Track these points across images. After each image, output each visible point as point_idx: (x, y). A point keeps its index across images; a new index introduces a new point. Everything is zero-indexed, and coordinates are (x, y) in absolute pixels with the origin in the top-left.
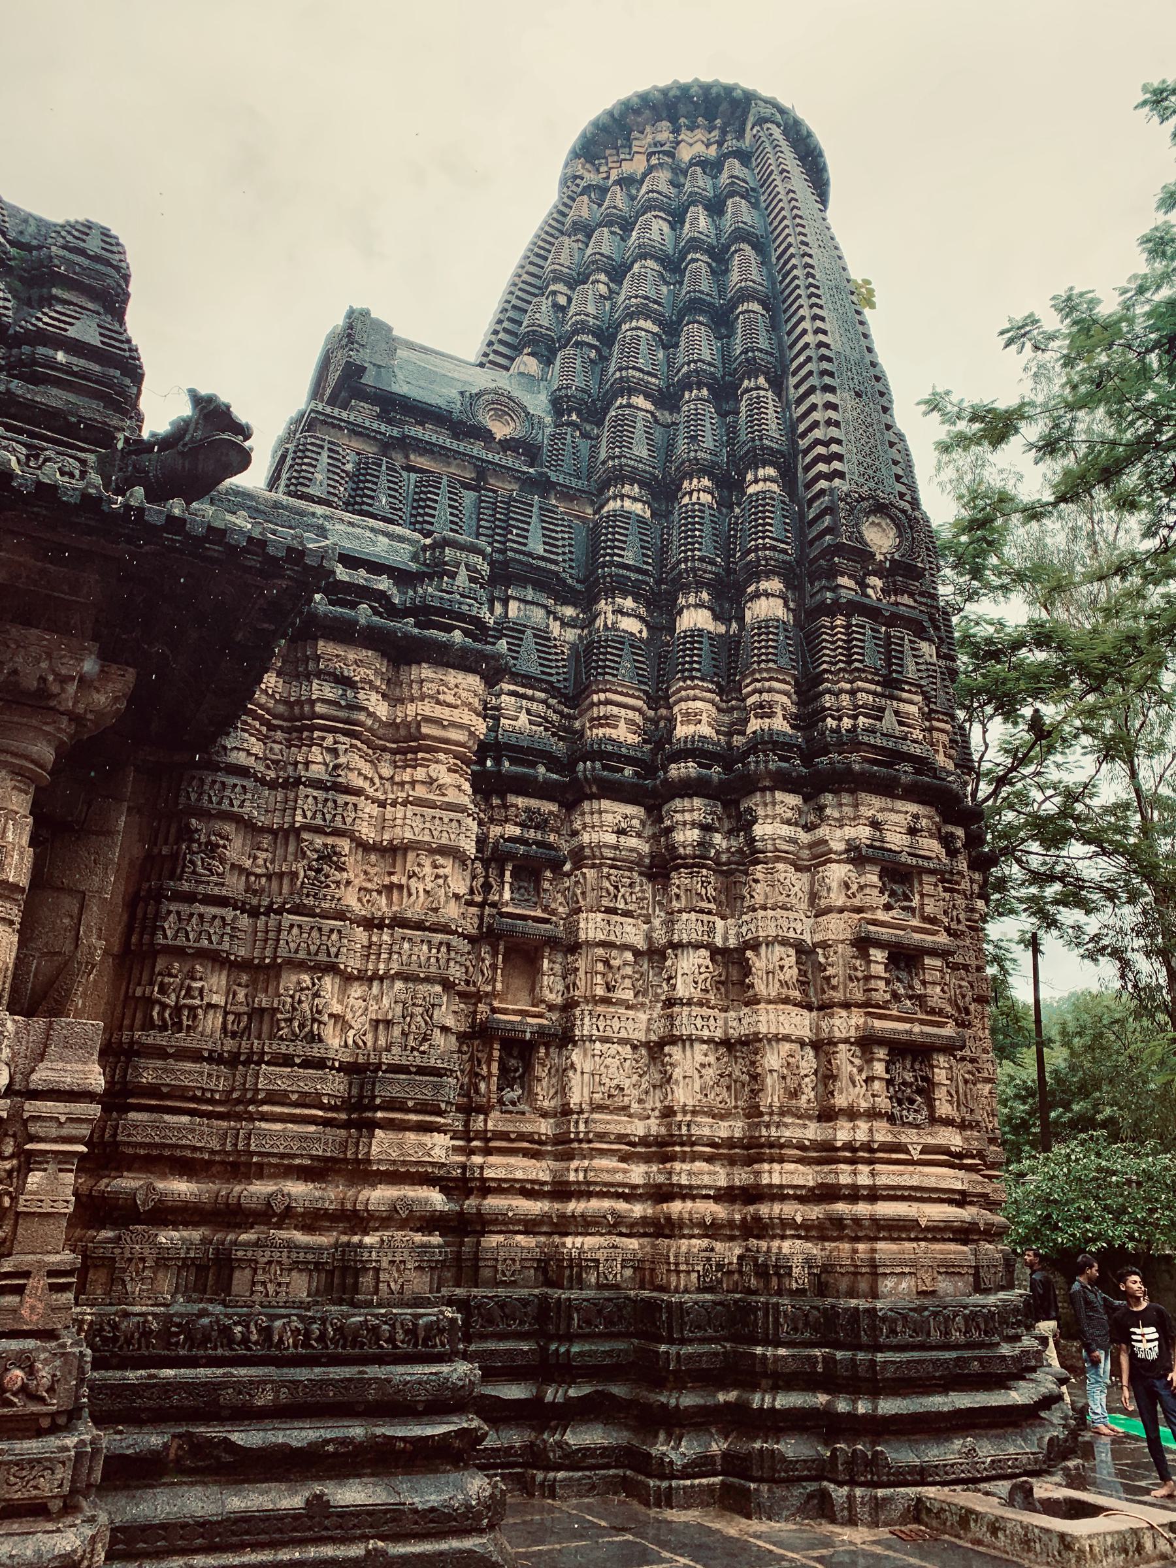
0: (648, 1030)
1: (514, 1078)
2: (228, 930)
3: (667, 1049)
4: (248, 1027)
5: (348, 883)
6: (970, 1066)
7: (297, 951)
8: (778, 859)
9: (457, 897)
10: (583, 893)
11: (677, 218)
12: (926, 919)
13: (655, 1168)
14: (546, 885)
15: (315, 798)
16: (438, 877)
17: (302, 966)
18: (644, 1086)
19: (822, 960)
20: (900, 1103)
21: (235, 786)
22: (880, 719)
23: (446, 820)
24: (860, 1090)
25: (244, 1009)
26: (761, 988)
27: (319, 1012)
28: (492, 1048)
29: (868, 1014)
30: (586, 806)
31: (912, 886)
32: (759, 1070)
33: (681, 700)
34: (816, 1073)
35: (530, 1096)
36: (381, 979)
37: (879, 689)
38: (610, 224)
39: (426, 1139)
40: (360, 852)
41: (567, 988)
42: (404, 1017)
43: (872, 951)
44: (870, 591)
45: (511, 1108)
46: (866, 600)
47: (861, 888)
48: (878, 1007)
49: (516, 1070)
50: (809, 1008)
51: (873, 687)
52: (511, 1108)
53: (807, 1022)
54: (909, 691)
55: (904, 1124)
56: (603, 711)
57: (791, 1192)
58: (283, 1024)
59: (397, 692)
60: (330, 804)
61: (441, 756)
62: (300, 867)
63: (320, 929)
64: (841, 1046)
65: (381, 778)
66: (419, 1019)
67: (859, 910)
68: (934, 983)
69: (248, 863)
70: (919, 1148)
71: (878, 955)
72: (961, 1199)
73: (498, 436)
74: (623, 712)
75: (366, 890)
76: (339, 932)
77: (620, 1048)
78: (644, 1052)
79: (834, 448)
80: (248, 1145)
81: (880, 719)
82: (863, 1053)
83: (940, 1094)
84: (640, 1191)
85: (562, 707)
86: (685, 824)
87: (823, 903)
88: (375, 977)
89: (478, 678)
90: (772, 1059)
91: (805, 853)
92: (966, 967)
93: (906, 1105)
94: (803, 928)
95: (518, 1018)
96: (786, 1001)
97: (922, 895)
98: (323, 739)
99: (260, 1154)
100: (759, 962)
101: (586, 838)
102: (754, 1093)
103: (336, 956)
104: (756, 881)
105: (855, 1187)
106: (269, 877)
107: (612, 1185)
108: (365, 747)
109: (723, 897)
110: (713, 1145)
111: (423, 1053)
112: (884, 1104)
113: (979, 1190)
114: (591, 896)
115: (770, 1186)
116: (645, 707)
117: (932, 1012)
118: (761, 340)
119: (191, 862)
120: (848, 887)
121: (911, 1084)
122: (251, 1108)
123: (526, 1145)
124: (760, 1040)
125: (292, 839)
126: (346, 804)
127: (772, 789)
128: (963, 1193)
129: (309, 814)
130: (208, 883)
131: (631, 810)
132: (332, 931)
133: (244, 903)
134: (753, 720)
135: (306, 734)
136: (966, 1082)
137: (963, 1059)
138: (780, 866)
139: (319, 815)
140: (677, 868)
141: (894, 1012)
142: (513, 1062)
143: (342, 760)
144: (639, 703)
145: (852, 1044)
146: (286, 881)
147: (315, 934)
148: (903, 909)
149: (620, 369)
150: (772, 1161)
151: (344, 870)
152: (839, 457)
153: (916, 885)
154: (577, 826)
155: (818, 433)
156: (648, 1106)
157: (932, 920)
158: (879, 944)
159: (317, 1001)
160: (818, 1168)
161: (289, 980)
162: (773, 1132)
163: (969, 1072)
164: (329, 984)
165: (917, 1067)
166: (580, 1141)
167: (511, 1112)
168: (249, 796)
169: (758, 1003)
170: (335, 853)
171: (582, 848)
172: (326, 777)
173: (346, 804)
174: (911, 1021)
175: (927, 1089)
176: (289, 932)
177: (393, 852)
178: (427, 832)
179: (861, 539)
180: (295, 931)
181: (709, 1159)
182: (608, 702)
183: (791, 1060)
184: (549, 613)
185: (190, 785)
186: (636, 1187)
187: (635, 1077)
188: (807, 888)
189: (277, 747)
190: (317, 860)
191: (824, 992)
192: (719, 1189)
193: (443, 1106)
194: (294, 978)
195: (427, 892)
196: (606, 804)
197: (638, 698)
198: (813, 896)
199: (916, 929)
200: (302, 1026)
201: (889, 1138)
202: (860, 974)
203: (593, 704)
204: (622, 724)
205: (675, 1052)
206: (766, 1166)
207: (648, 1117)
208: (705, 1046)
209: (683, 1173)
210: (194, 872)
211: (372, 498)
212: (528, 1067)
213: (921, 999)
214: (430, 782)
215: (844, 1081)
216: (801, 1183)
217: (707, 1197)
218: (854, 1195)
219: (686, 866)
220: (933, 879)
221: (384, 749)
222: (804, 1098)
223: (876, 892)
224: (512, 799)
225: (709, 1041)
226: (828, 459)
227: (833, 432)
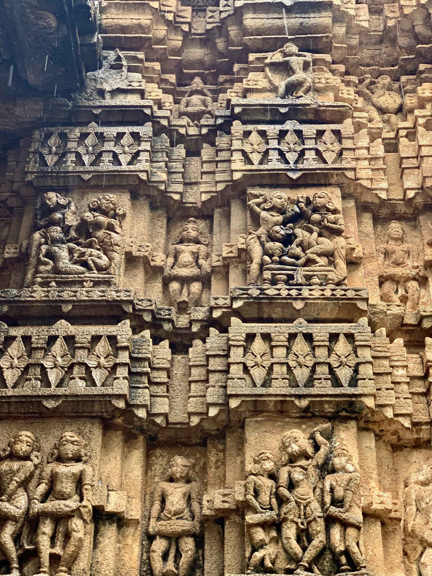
2: (124, 357)
7: (266, 384)
21: (120, 136)
27: (336, 502)
40: (367, 219)
63: (308, 337)
65: (382, 111)
75: (391, 278)
76: (350, 337)
103: (353, 382)
119: (50, 255)
129: (256, 158)
130: (81, 283)
132: (334, 337)
135: (236, 67)
139: (274, 155)
143: (299, 75)
151: (338, 233)
159: (329, 480)
168: (145, 146)
172: (279, 101)
176: (246, 350)
185: (44, 143)
189: (196, 99)
190: (284, 223)
210: (56, 270)
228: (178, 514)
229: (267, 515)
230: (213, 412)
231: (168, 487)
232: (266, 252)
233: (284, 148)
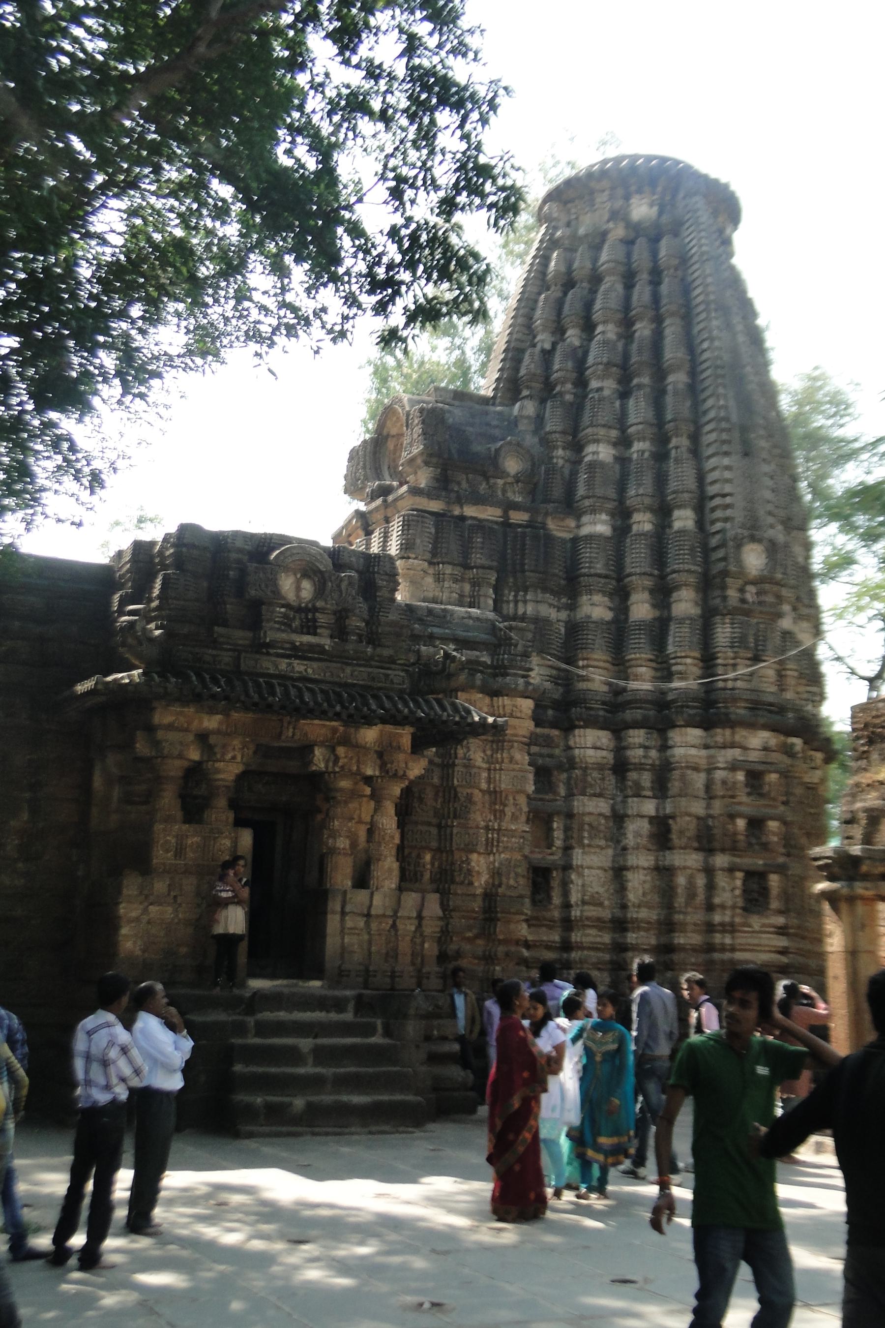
0: (613, 861)
8: (687, 767)
22: (750, 681)
30: (577, 731)
46: (746, 606)
71: (741, 823)
72: (783, 952)
79: (728, 500)
81: (750, 681)
105: (723, 944)
112: (740, 902)
158: (741, 815)
175: (765, 891)
182: (588, 666)
196: (589, 731)
212: (548, 882)
218: (723, 949)
219: (635, 769)
226: (727, 507)
227: (728, 489)
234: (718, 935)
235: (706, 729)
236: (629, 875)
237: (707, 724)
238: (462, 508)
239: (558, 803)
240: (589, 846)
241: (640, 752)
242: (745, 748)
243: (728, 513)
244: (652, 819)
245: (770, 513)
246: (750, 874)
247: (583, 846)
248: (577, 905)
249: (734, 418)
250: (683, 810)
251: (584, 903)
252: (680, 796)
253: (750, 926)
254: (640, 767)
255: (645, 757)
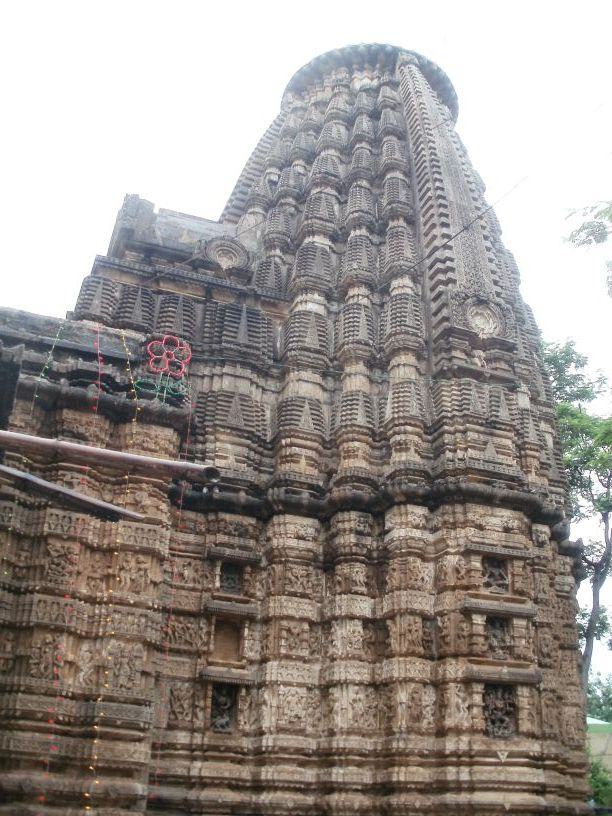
1: (224, 710)
3: (330, 690)
4: (13, 668)
5: (79, 573)
6: (551, 695)
8: (410, 554)
9: (155, 584)
10: (273, 582)
11: (350, 123)
12: (516, 592)
13: (322, 771)
14: (247, 577)
15: (57, 515)
16: (140, 569)
17: (44, 628)
18: (318, 715)
19: (440, 624)
20: (493, 722)
23: (146, 530)
24: (464, 714)
25: (11, 656)
26: (395, 645)
28: (207, 689)
29: (471, 661)
30: (276, 519)
31: (506, 570)
32: (392, 704)
33: (344, 441)
34: (435, 703)
35: (237, 722)
36: (102, 638)
37: (482, 429)
38: (308, 130)
39: (131, 747)
40: (88, 552)
41: (262, 648)
42: (116, 665)
43: (474, 617)
44: (476, 360)
45: (220, 729)
46: (473, 367)
47: (469, 571)
48: (477, 655)
49: (226, 704)
50: (432, 658)
51: (478, 427)
52: (220, 729)
53: (429, 669)
54: (505, 430)
55: (495, 737)
56: (288, 451)
57: (413, 786)
58: (33, 667)
59: (117, 443)
60: (66, 520)
61: (144, 486)
62: (45, 562)
64: (452, 685)
66: (126, 666)
67: (467, 588)
68: (520, 637)
69: (14, 559)
70: (506, 754)
71: (479, 620)
72: (541, 790)
73: (224, 267)
74: (304, 452)
75: (91, 578)
77: (298, 690)
78: (317, 692)
79: (448, 263)
80: (9, 746)
82: (466, 688)
83: (523, 715)
84: (313, 787)
85: (261, 449)
86: (345, 530)
87: (441, 584)
88: (96, 638)
89: (171, 431)
90: (402, 696)
91: (431, 549)
92: (549, 625)
93: (498, 724)
94: (425, 603)
95: (226, 669)
96: (414, 654)
97: (513, 575)
98: (64, 475)
99: (16, 753)
100: (395, 629)
101: (275, 542)
102: (390, 719)
103: (69, 622)
104: (394, 570)
105: (458, 782)
106: (28, 568)
107: (291, 782)
108: (92, 480)
109: (373, 582)
110: (361, 755)
111: (129, 689)
112: (480, 724)
113: (556, 782)
114: (279, 583)
115: (399, 782)
116: (321, 448)
117: (519, 657)
118: (400, 196)
120: (458, 571)
121: (502, 710)
122: (12, 722)
123: (232, 755)
124: (394, 682)
125: (43, 543)
126: (78, 519)
127: (405, 503)
128: (544, 786)
129: (53, 527)
131: (309, 521)
133: (10, 586)
134: (394, 454)
136: (547, 706)
137: (545, 690)
138: (411, 559)
140: (340, 563)
141: (491, 659)
142: (223, 699)
144: (316, 445)
145: (458, 682)
146: (38, 571)
147: (55, 606)
148: (499, 586)
149: (307, 219)
150: (401, 765)
152: (452, 270)
153: (509, 567)
154: (270, 534)
155: (438, 254)
156: (320, 729)
157: (521, 593)
160: (435, 769)
161: (38, 638)
162: (402, 745)
163: (550, 699)
164: (65, 643)
165: (507, 696)
166: (270, 753)
167: (220, 733)
169: (393, 656)
170: (70, 553)
171: (272, 550)
173: (78, 519)
174: (502, 665)
175: (513, 711)
177: (108, 551)
178: (132, 539)
179: (466, 324)
180: (42, 604)
181: (360, 765)
182: (292, 445)
183: (415, 695)
184: (252, 383)
186: (310, 784)
187: (311, 709)
188: (432, 574)
191: (441, 647)
192: (366, 785)
193: (142, 725)
194: (41, 636)
195: (132, 580)
196: (289, 518)
197: (315, 441)
198: (437, 579)
199: (507, 600)
200: (46, 668)
201: (484, 748)
202: (465, 634)
203: (282, 447)
204: (303, 461)
205: (336, 692)
206: (396, 769)
207: (320, 737)
208: (357, 688)
209: (338, 774)
211: (130, 313)
212: (235, 703)
213: (510, 649)
214: (136, 504)
215: (452, 709)
216: (420, 780)
217: (357, 790)
218: (458, 787)
219: (346, 561)
220: (521, 563)
221: (107, 482)
222: (425, 721)
223: (479, 574)
224: (223, 516)
225: (360, 684)
226: (445, 271)
228: (9, 652)
229: (36, 661)
230: (24, 624)
231: (7, 642)
232: (50, 568)
233: (64, 524)
234: (452, 769)
235: (432, 510)
236: (336, 692)
237: (434, 500)
238: (158, 284)
239: (253, 606)
240: (288, 657)
241: (352, 539)
242: (480, 527)
243: (450, 275)
244: (367, 622)
245: (496, 283)
246: (492, 686)
247: (279, 657)
248: (271, 732)
249: (451, 198)
250: (403, 606)
251: (280, 730)
252: (399, 589)
253: (497, 756)
254: (351, 558)
255: (356, 545)
